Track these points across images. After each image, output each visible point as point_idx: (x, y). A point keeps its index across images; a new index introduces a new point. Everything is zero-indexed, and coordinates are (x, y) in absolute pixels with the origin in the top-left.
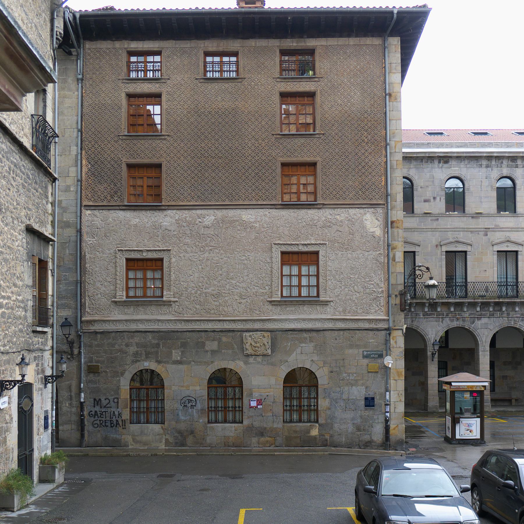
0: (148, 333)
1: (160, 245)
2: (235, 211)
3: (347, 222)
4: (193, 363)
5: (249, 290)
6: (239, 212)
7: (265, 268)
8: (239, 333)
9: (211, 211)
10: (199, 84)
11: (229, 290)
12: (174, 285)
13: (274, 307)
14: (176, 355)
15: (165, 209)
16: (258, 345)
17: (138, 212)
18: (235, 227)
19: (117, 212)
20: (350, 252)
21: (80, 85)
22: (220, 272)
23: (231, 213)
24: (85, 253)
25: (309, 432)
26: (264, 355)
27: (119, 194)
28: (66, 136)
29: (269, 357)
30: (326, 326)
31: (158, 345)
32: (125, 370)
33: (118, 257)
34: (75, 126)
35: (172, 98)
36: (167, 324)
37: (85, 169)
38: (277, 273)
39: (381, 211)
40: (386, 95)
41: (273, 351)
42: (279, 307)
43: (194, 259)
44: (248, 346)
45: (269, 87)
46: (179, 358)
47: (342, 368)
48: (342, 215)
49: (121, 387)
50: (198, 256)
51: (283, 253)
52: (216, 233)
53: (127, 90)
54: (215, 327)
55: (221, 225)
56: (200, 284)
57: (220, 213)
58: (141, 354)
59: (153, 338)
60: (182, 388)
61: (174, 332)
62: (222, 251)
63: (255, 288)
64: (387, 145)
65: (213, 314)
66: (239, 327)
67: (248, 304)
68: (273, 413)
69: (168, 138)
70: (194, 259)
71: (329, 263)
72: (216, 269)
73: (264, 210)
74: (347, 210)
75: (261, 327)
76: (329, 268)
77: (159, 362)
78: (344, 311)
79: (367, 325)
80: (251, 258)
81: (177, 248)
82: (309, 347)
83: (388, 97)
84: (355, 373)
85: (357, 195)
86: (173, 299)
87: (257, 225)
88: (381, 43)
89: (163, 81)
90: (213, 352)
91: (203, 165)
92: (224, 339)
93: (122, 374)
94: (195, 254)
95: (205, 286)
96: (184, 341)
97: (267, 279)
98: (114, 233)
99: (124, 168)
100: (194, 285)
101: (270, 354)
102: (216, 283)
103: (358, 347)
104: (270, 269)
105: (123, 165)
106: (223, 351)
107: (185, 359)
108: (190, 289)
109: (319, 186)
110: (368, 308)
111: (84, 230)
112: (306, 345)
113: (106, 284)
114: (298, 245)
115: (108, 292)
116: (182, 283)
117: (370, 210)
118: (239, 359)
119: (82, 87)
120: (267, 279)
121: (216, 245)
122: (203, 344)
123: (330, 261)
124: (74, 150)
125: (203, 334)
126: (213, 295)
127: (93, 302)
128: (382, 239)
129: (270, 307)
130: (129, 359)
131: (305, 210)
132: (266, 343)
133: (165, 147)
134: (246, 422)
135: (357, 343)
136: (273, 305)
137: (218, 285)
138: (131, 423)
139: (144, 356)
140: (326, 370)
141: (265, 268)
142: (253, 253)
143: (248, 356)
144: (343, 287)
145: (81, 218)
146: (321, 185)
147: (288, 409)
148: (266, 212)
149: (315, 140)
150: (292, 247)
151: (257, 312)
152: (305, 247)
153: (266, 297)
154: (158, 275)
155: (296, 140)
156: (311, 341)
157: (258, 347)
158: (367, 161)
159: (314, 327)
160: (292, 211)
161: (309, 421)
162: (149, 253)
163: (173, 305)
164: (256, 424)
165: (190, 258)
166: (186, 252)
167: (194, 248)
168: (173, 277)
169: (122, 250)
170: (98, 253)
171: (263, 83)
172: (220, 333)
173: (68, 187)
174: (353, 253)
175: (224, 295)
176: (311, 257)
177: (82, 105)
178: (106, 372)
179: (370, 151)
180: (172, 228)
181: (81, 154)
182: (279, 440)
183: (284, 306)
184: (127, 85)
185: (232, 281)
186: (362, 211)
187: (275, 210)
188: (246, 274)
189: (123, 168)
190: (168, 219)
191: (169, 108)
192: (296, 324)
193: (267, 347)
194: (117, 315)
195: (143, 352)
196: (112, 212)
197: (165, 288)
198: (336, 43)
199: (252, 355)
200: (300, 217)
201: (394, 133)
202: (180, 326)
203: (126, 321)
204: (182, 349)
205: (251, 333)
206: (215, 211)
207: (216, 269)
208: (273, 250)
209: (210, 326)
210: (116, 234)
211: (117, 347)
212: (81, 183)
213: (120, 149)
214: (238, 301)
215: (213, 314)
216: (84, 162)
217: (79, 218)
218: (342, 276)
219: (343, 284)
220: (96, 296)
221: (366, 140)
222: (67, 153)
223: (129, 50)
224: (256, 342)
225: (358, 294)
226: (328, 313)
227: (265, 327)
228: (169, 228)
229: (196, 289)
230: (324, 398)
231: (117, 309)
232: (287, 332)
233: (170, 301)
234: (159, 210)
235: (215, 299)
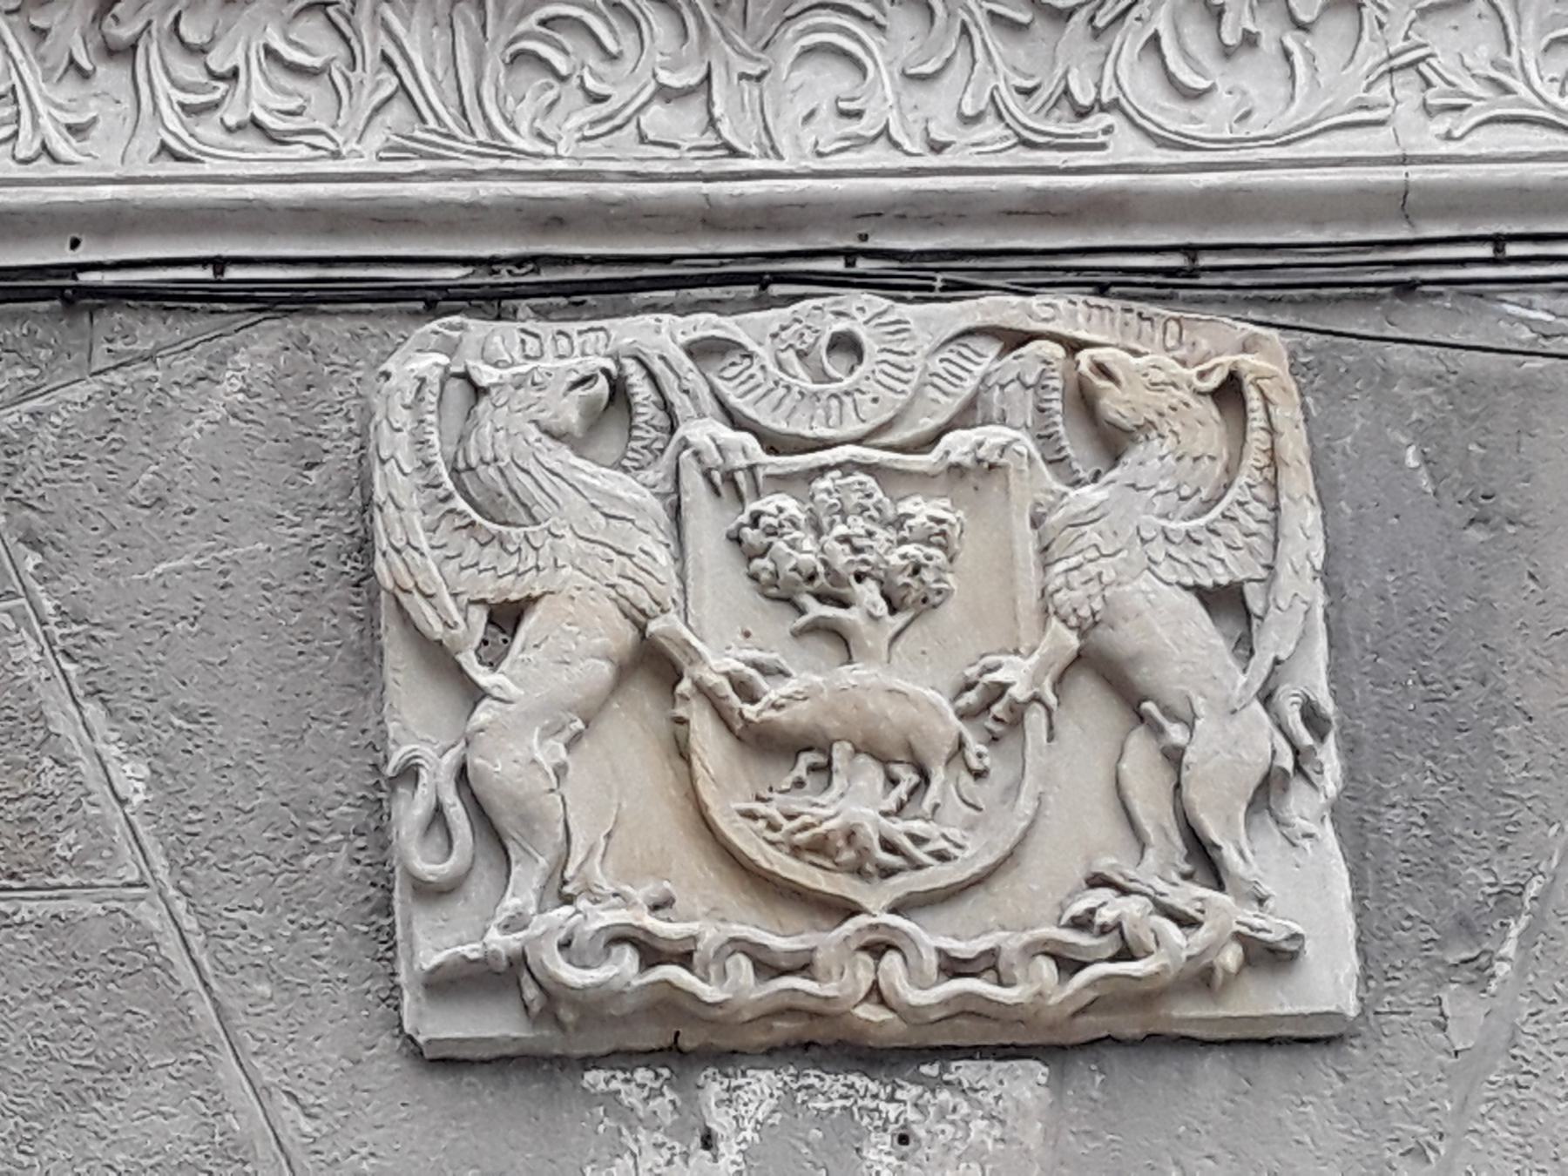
16: (903, 681)
41: (1423, 911)
44: (526, 719)
75: (984, 159)
132: (1175, 641)
157: (905, 761)
193: (1231, 746)
199: (686, 1044)
224: (814, 603)
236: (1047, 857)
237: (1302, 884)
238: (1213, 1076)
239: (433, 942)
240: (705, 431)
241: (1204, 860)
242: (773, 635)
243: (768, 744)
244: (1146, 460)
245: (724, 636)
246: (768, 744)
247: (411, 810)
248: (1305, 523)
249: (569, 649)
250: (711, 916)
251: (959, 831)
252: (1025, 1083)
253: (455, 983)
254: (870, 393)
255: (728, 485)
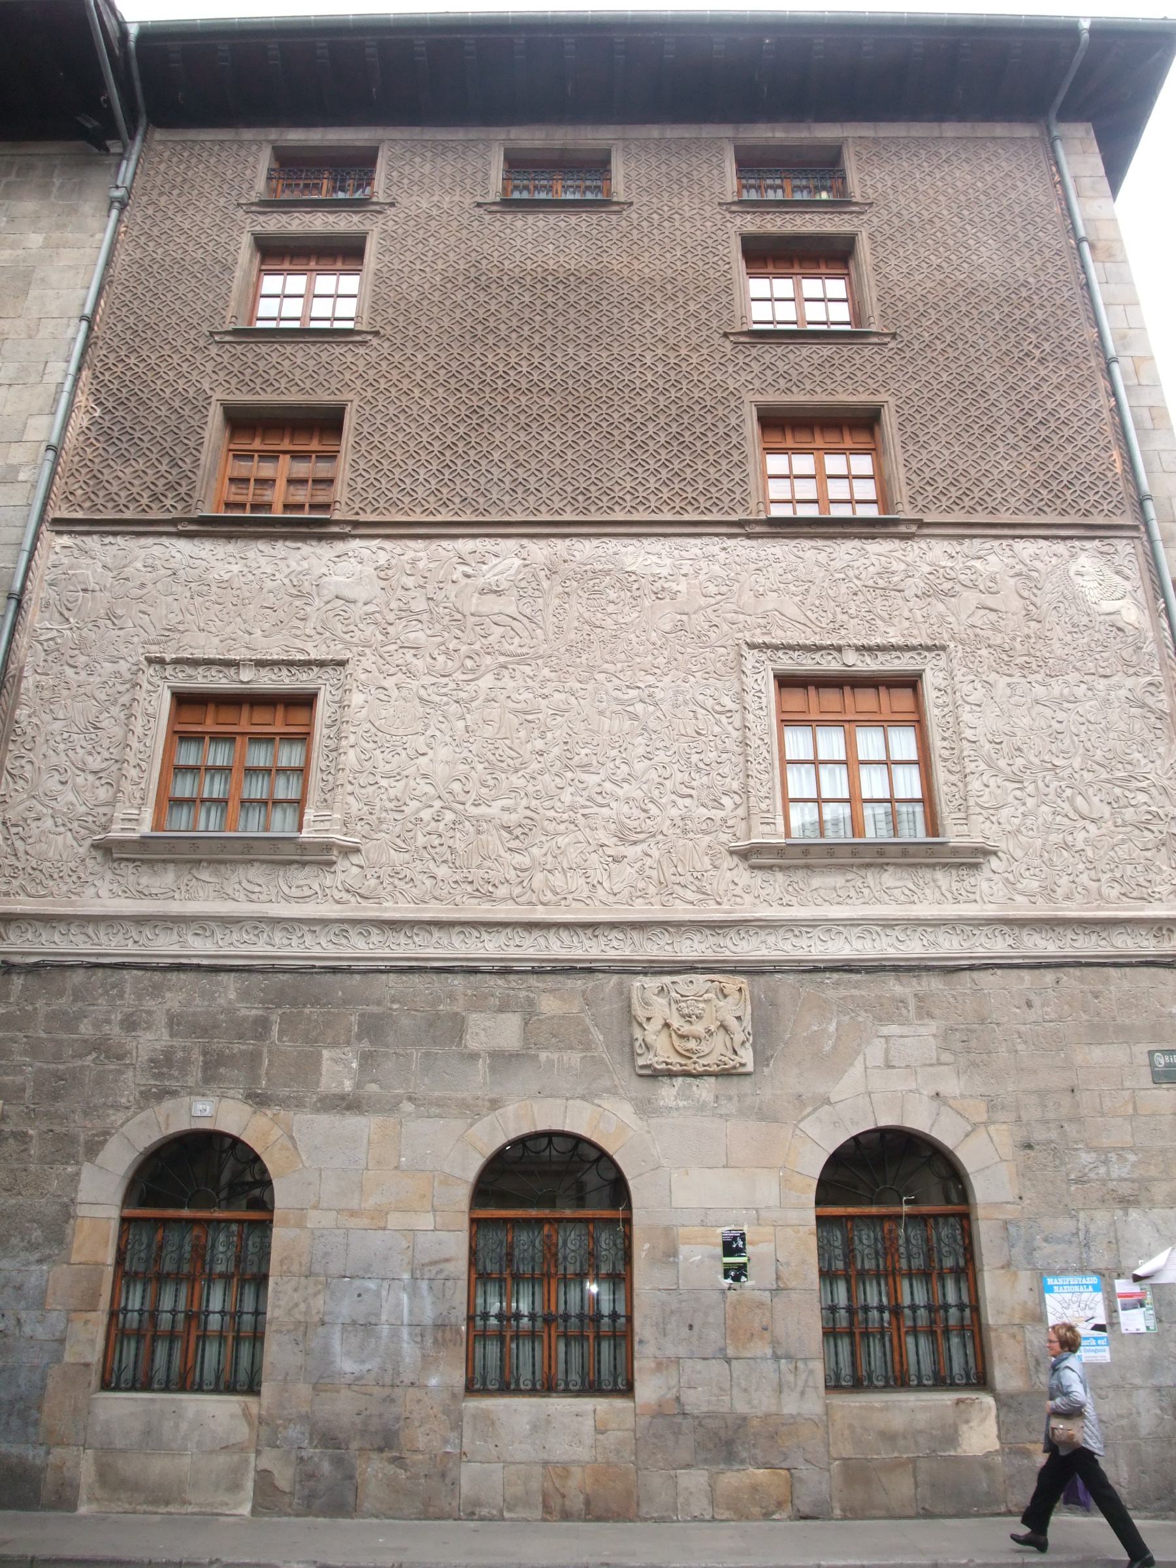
0: (223, 977)
1: (309, 646)
2: (596, 542)
3: (1012, 581)
4: (407, 1107)
5: (654, 810)
6: (612, 545)
7: (717, 730)
8: (615, 978)
9: (512, 544)
10: (487, 217)
11: (572, 808)
12: (349, 788)
13: (760, 875)
14: (338, 1069)
15: (343, 537)
16: (698, 1028)
17: (241, 544)
18: (595, 592)
19: (165, 540)
20: (1039, 677)
21: (114, 213)
22: (539, 744)
23: (585, 549)
24: (21, 670)
25: (951, 1437)
26: (726, 1074)
27: (183, 490)
28: (40, 336)
29: (746, 1083)
30: (980, 951)
31: (261, 1027)
32: (106, 1133)
33: (145, 685)
34: (75, 312)
35: (398, 246)
36: (308, 938)
37: (80, 420)
38: (763, 749)
39: (1129, 549)
40: (1079, 241)
41: (761, 1058)
42: (780, 876)
43: (437, 699)
45: (708, 224)
46: (348, 1086)
47: (1071, 1129)
48: (992, 558)
49: (81, 1211)
50: (452, 685)
51: (785, 682)
52: (528, 612)
53: (258, 228)
54: (512, 952)
55: (546, 584)
56: (456, 787)
57: (539, 551)
58: (187, 1061)
59: (245, 995)
60: (353, 1222)
61: (335, 970)
62: (546, 672)
63: (680, 801)
64: (1108, 363)
65: (504, 900)
66: (612, 954)
67: (649, 862)
68: (775, 1343)
69: (375, 341)
70: (437, 699)
71: (966, 717)
72: (523, 734)
73: (705, 540)
74: (1005, 542)
75: (710, 955)
76: (968, 733)
77: (258, 1100)
78: (1048, 892)
79: (1149, 946)
80: (659, 694)
81: (373, 659)
82: (918, 1039)
83: (1085, 246)
84: (1131, 1149)
85: (1035, 501)
86: (338, 837)
87: (683, 587)
88: (1037, 134)
89: (377, 208)
90: (502, 1060)
91: (487, 410)
92: (549, 1005)
93: (93, 1148)
94: (444, 680)
95: (473, 795)
96: (374, 1009)
97: (725, 769)
98: (143, 607)
99: (215, 417)
100: (430, 790)
101: (750, 1068)
102: (517, 781)
103: (1126, 1035)
104: (735, 734)
105: (212, 409)
106: (543, 1056)
107: (373, 1088)
108: (414, 804)
109: (899, 474)
110: (1141, 880)
111: (38, 592)
112: (905, 1030)
113: (80, 780)
114: (839, 649)
115: (83, 809)
116: (384, 783)
117: (1088, 544)
118: (613, 1091)
119: (119, 221)
120: (725, 769)
121: (524, 650)
122: (457, 1028)
123: (967, 708)
124: (61, 371)
125: (457, 981)
126: (507, 828)
127: (19, 844)
128: (1150, 634)
129: (744, 876)
130: (132, 1081)
131: (856, 543)
132: (733, 1023)
133: (361, 363)
134: (648, 1389)
135: (1119, 1021)
136: (753, 867)
137: (530, 789)
138: (105, 1386)
139: (195, 1075)
140: (1003, 1136)
141: (717, 730)
142: (667, 679)
143: (655, 1075)
144: (1031, 802)
145: (30, 559)
146: (902, 471)
147: (845, 1328)
148: (714, 546)
149: (867, 352)
150: (817, 656)
151: (690, 895)
152: (868, 659)
153: (724, 838)
154: (290, 756)
155: (805, 351)
156: (924, 1012)
157: (698, 1039)
158: (1050, 405)
159: (932, 952)
160: (807, 543)
161: (942, 1382)
162: (264, 672)
163: (342, 864)
164: (698, 1400)
165: (422, 692)
166: (411, 674)
167: (441, 659)
168: (351, 758)
169: (161, 662)
170: (69, 672)
171: (687, 215)
172: (533, 980)
173: (15, 469)
174: (1053, 681)
175: (551, 827)
176: (895, 690)
177: (108, 264)
178: (22, 1137)
179: (1055, 379)
180: (360, 593)
181: (76, 380)
182: (816, 1482)
183: (800, 873)
184: (262, 218)
185: (585, 777)
186: (1060, 547)
187: (747, 543)
188: (641, 751)
189: (209, 419)
190: (350, 565)
191: (385, 269)
192: (859, 945)
193: (739, 1037)
194: (106, 895)
195: (197, 1057)
196: (150, 541)
197: (313, 796)
198: (903, 134)
199: (671, 1075)
200: (837, 564)
201: (1123, 337)
202: (359, 947)
203: (141, 920)
204: (365, 1045)
205: (667, 979)
206: (525, 541)
207: (523, 734)
208: (748, 665)
209: (490, 947)
210: (150, 610)
211: (86, 1029)
212: (57, 456)
213: (209, 369)
214: (609, 851)
215: (504, 900)
216: (81, 399)
217: (25, 556)
218: (1020, 762)
219: (1031, 789)
220: (34, 825)
221: (1037, 352)
222: (33, 379)
223: (279, 144)
224: (687, 1018)
225: (1092, 828)
226: (986, 894)
227: (727, 954)
228: (348, 593)
229: (438, 804)
230: (1007, 1265)
231: (109, 876)
232: (818, 977)
233: (328, 847)
234: (320, 538)
235: (514, 844)
236: (715, 1052)
237: (747, 1056)
238: (735, 1079)
239: (641, 1061)
240: (674, 994)
241: (735, 1052)
242: (682, 1022)
243: (682, 1037)
244: (729, 999)
245: (676, 1022)
246: (682, 1037)
247: (637, 1044)
248: (749, 1007)
249: (656, 1025)
250: (675, 1059)
251: (704, 1048)
252: (713, 1079)
253: (642, 1067)
254: (693, 989)
255: (677, 1002)
